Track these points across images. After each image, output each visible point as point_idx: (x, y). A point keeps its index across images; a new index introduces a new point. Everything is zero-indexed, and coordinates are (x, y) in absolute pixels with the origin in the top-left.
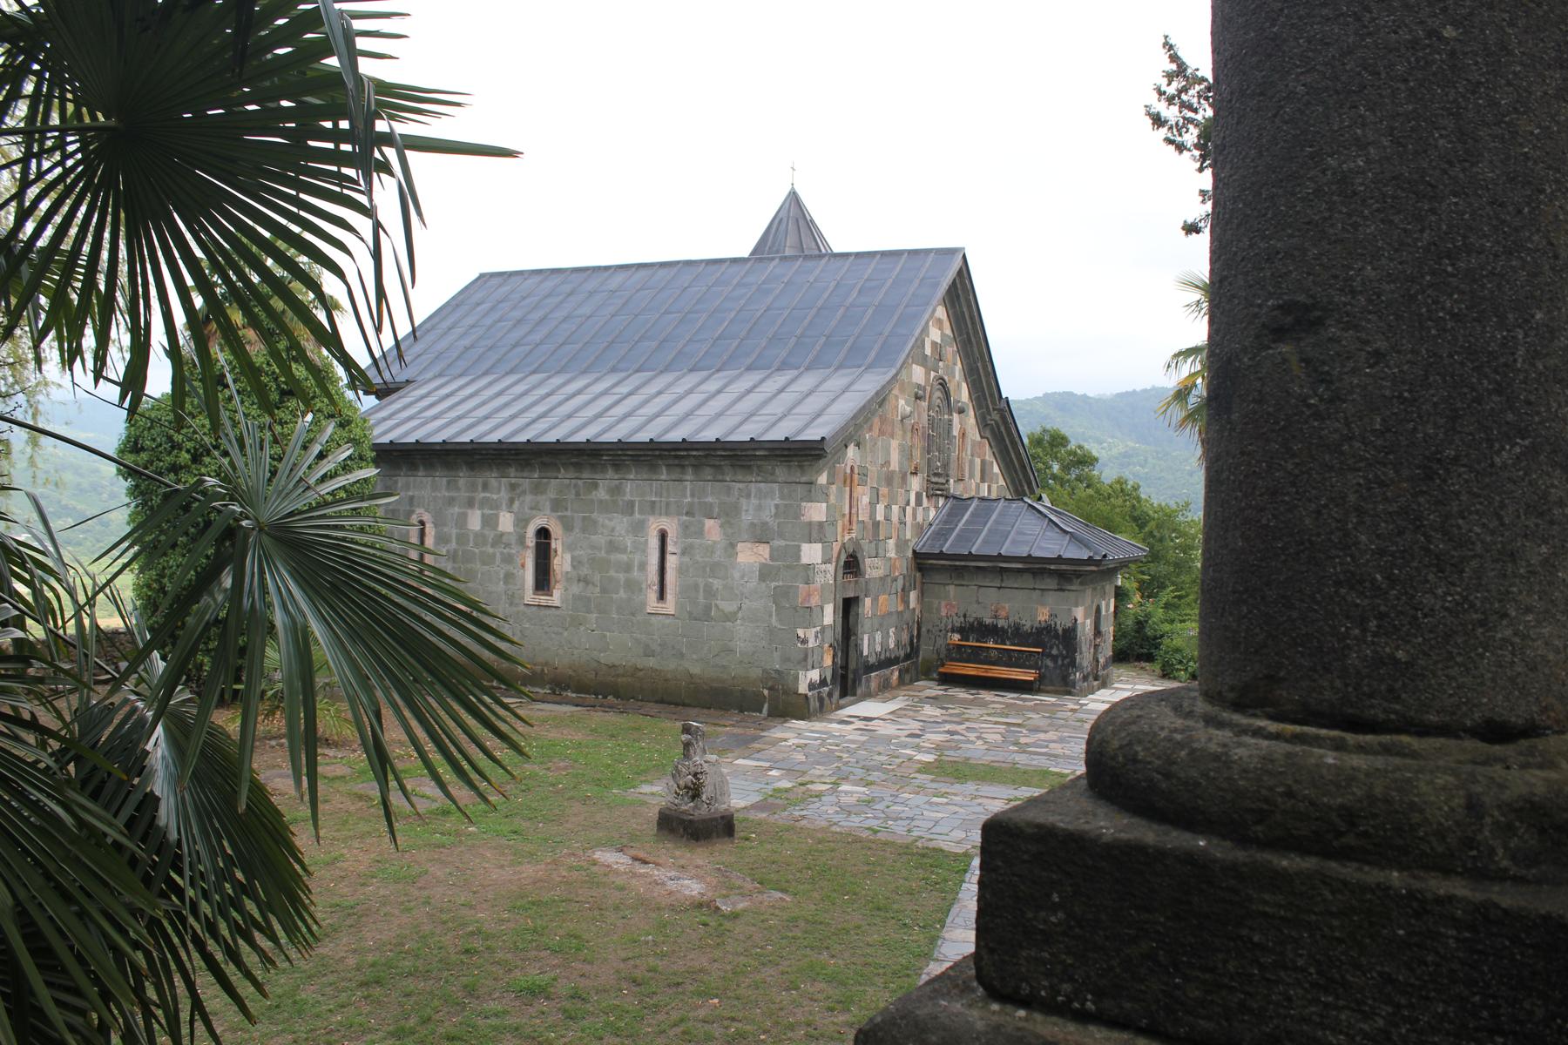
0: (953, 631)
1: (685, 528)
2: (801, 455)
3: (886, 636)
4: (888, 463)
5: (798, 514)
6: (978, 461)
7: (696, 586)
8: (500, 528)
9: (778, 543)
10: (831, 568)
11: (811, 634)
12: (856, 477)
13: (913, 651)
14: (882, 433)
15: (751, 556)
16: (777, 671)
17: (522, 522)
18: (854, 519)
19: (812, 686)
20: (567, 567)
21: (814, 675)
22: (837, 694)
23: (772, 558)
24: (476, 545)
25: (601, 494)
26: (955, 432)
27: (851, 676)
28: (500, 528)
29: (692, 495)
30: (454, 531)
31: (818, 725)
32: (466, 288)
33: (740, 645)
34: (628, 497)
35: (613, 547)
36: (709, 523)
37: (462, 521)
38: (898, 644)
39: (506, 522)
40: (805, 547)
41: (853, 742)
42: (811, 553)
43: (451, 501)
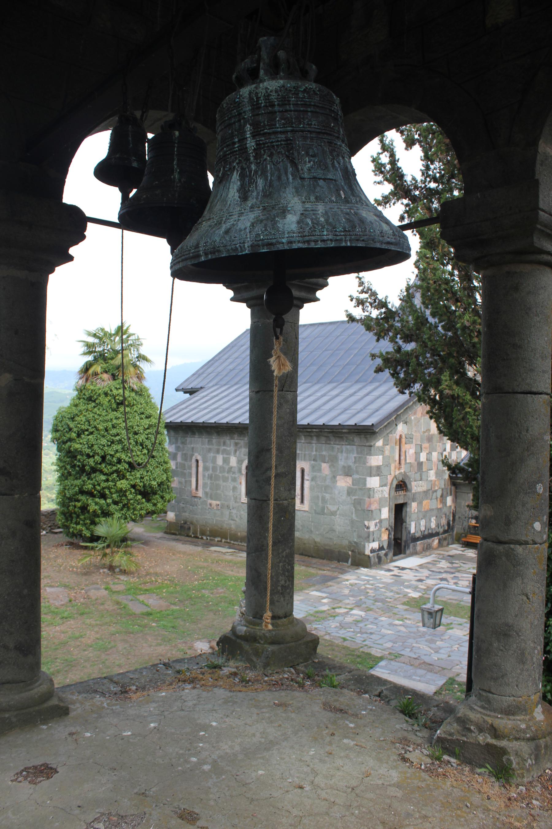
0: (472, 518)
1: (313, 467)
2: (364, 433)
4: (429, 430)
7: (318, 497)
8: (231, 464)
10: (386, 489)
12: (403, 440)
13: (450, 528)
16: (355, 542)
18: (403, 462)
19: (372, 551)
22: (391, 554)
23: (353, 484)
24: (220, 472)
27: (403, 544)
28: (231, 464)
29: (316, 451)
30: (211, 465)
31: (372, 572)
32: (239, 337)
33: (338, 528)
36: (324, 466)
37: (214, 460)
38: (438, 525)
40: (368, 479)
41: (383, 583)
42: (373, 482)
43: (210, 450)
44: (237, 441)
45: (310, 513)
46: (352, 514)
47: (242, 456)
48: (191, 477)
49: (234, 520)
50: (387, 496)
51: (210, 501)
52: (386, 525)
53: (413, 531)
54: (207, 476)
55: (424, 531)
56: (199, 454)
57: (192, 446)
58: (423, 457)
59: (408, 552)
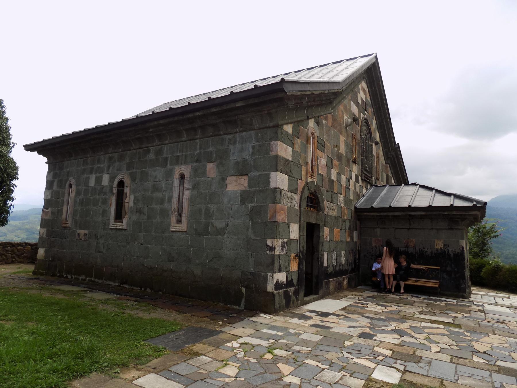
3: (339, 256)
4: (337, 146)
5: (268, 150)
6: (385, 175)
7: (200, 210)
8: (103, 184)
9: (255, 174)
10: (297, 197)
11: (278, 243)
14: (333, 126)
15: (236, 185)
16: (252, 273)
17: (112, 180)
19: (278, 286)
20: (131, 204)
21: (281, 277)
22: (302, 294)
23: (250, 186)
25: (151, 156)
26: (374, 154)
27: (314, 280)
28: (103, 184)
29: (200, 148)
30: (83, 188)
31: (279, 320)
34: (165, 156)
35: (156, 188)
38: (347, 261)
39: (106, 180)
40: (273, 174)
41: (305, 343)
42: (280, 180)
43: (84, 171)
44: (111, 155)
45: (188, 234)
46: (248, 230)
47: (115, 171)
48: (63, 206)
49: (101, 252)
50: (297, 208)
51: (78, 231)
52: (295, 248)
53: (325, 264)
54: (78, 202)
55: (336, 266)
56: (74, 178)
57: (68, 170)
58: (334, 177)
59: (321, 292)
